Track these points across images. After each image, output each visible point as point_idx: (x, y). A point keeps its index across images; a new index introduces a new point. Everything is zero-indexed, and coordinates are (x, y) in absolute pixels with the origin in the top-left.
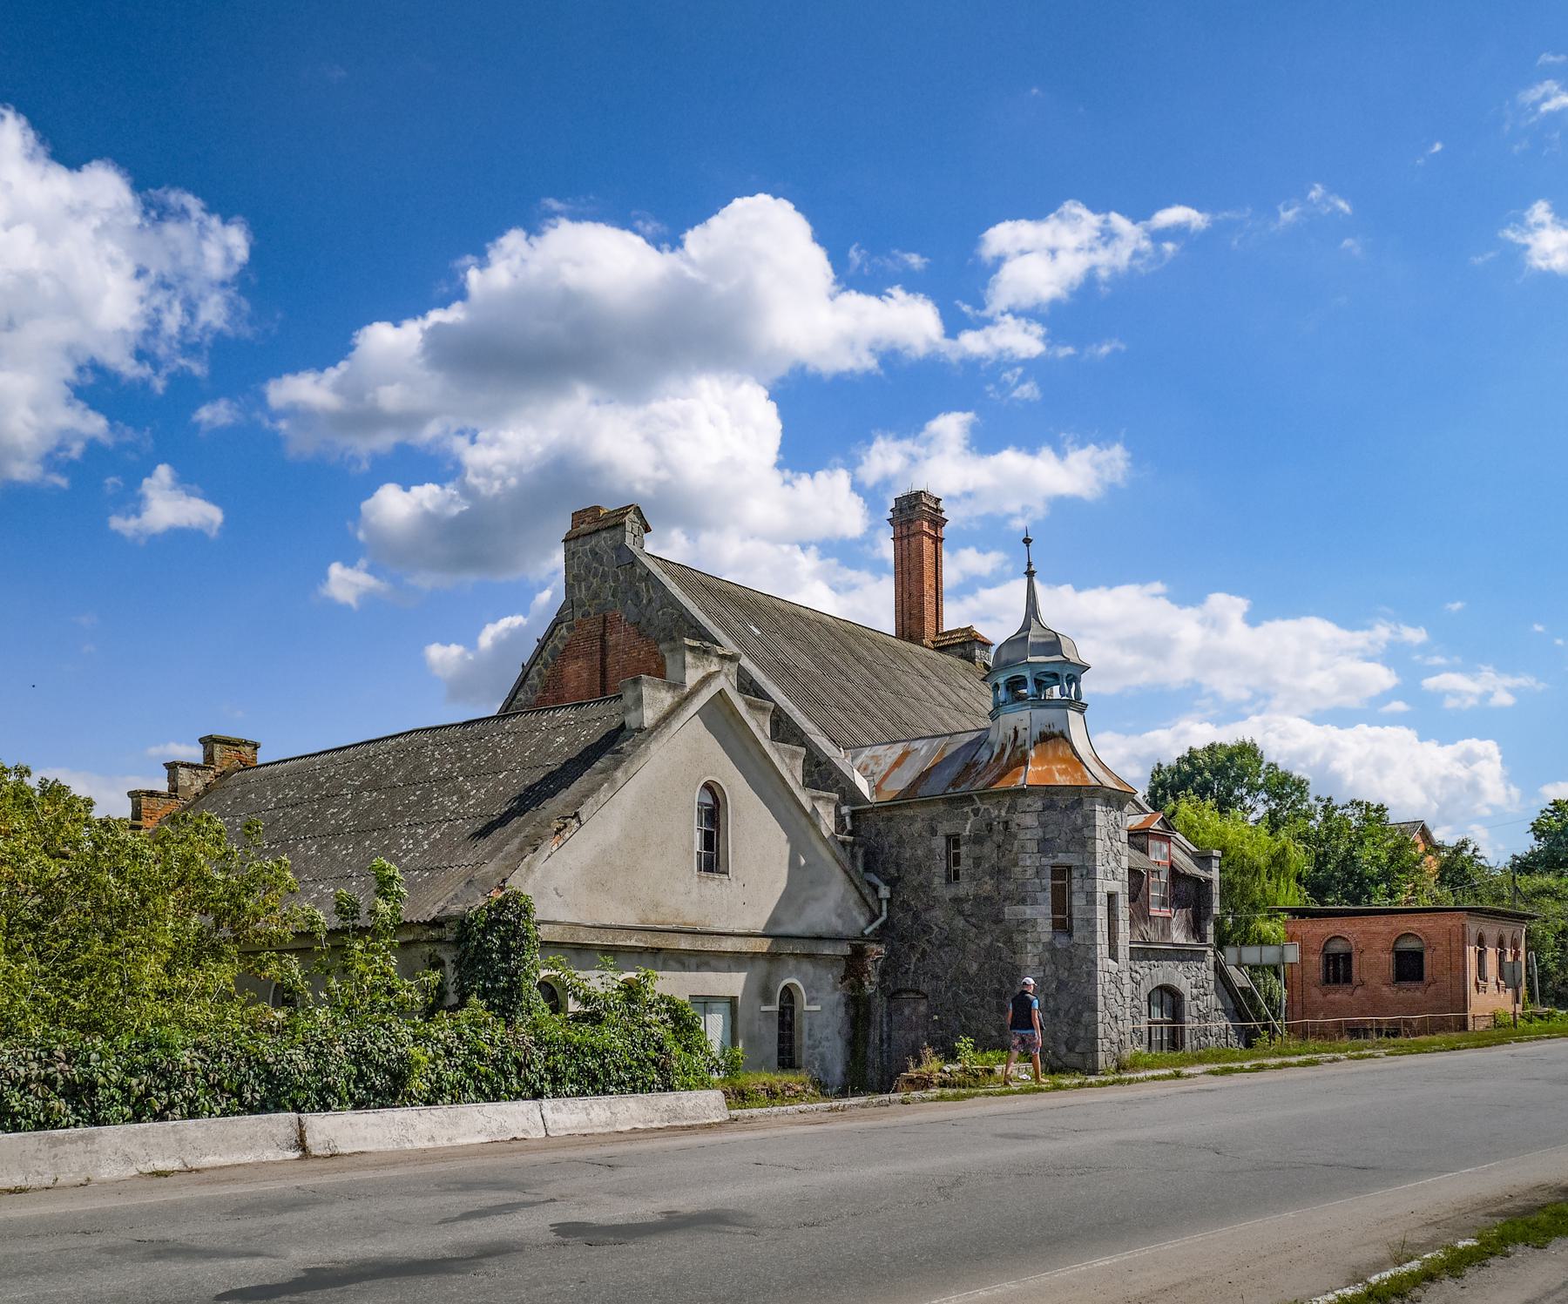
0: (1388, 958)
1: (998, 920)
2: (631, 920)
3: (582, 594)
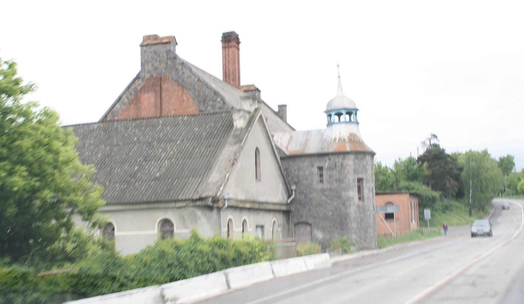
1: (339, 197)
3: (149, 67)
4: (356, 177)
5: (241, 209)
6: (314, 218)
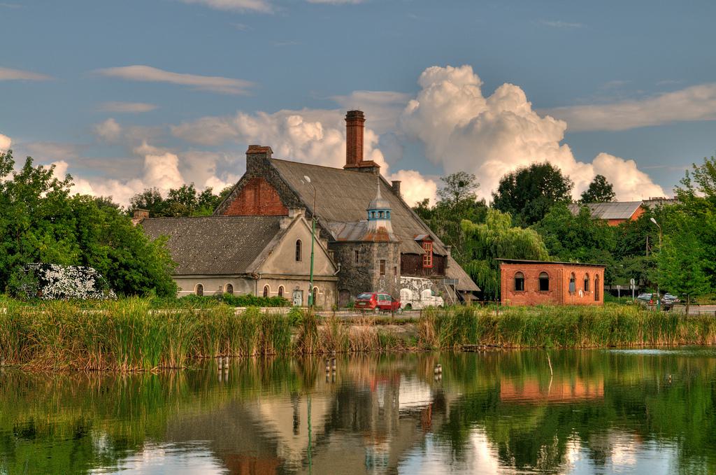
0: (537, 281)
2: (281, 273)
6: (351, 286)
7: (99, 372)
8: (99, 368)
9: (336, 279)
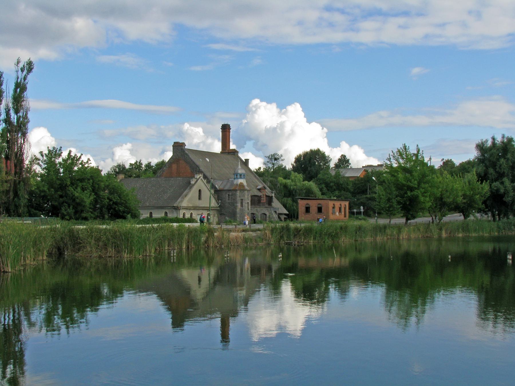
1: (234, 205)
2: (191, 206)
4: (240, 198)
5: (187, 209)
7: (113, 258)
8: (113, 256)
9: (218, 208)
